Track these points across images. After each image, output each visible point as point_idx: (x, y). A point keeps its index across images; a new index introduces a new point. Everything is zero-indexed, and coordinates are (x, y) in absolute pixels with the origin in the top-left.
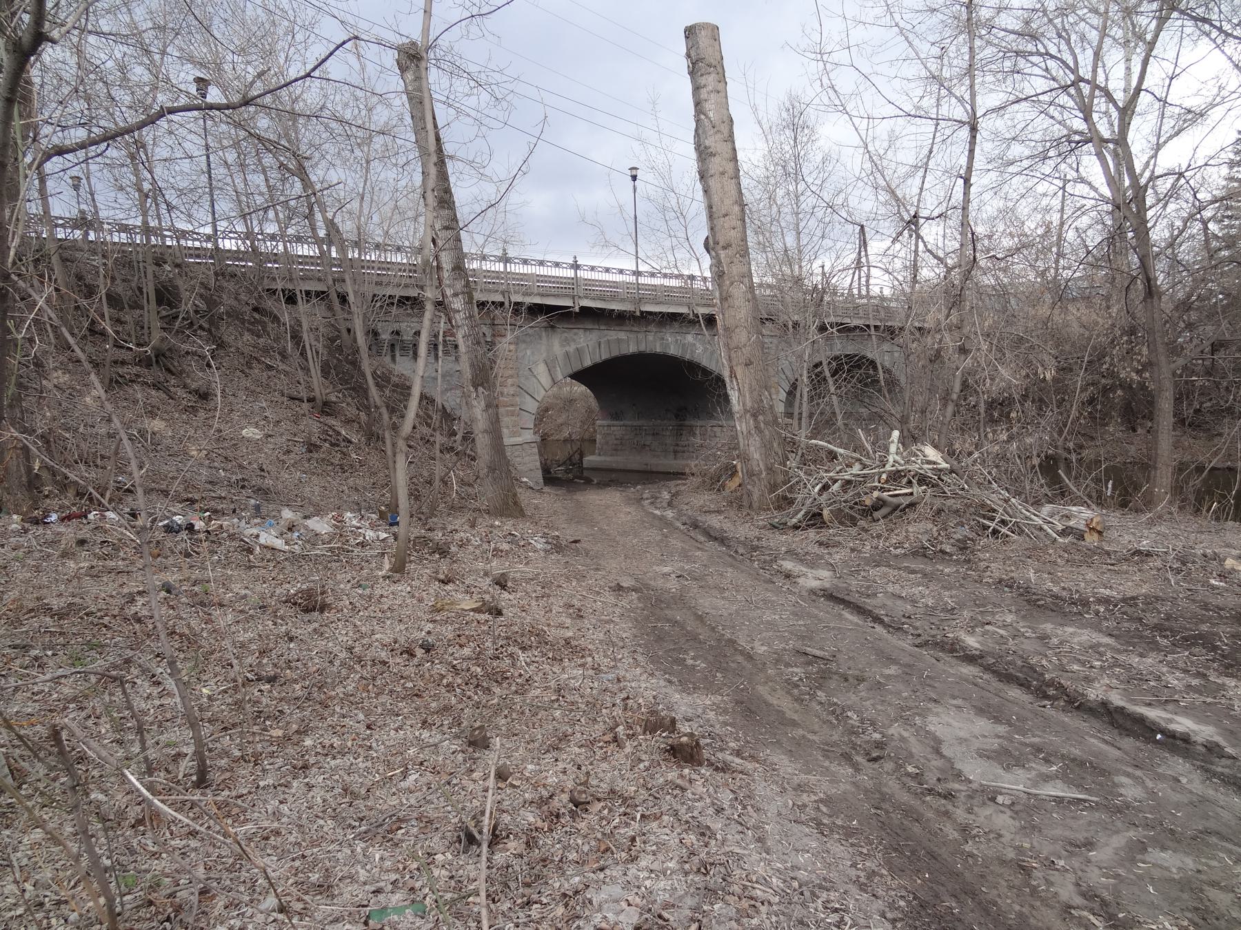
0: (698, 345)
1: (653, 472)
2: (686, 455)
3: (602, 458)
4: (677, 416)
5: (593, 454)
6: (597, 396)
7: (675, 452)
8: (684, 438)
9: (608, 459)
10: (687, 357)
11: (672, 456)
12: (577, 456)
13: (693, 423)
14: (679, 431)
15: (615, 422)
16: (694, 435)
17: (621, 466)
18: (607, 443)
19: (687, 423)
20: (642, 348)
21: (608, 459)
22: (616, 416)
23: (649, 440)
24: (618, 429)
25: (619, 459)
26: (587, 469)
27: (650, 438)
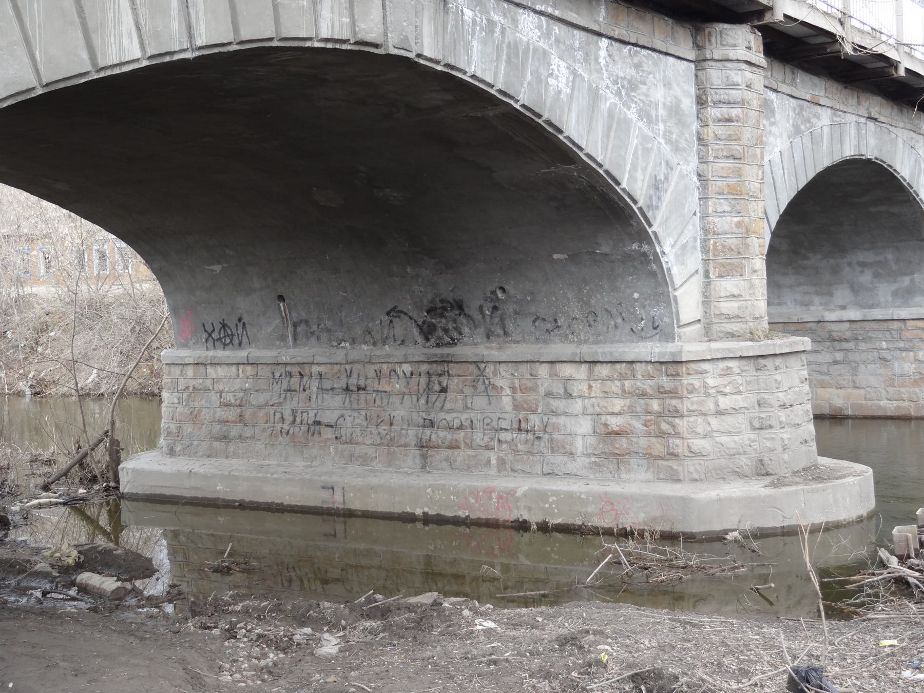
0: (557, 64)
1: (349, 514)
2: (461, 456)
3: (181, 465)
4: (427, 331)
5: (151, 443)
6: (162, 275)
7: (424, 446)
8: (453, 400)
9: (199, 466)
10: (524, 97)
11: (412, 458)
12: (102, 455)
13: (489, 351)
14: (435, 381)
15: (221, 354)
16: (491, 390)
17: (242, 492)
18: (194, 417)
19: (463, 351)
20: (370, 28)
21: (199, 466)
22: (224, 334)
23: (332, 407)
24: (228, 374)
25: (235, 466)
26: (134, 498)
27: (337, 400)
